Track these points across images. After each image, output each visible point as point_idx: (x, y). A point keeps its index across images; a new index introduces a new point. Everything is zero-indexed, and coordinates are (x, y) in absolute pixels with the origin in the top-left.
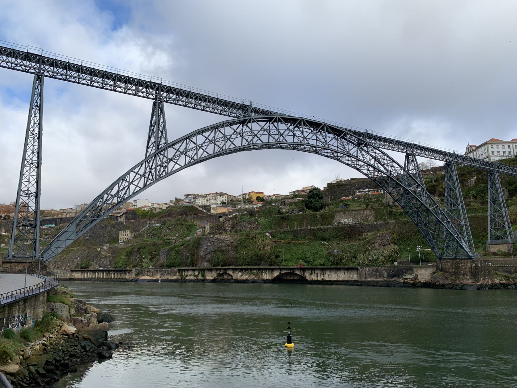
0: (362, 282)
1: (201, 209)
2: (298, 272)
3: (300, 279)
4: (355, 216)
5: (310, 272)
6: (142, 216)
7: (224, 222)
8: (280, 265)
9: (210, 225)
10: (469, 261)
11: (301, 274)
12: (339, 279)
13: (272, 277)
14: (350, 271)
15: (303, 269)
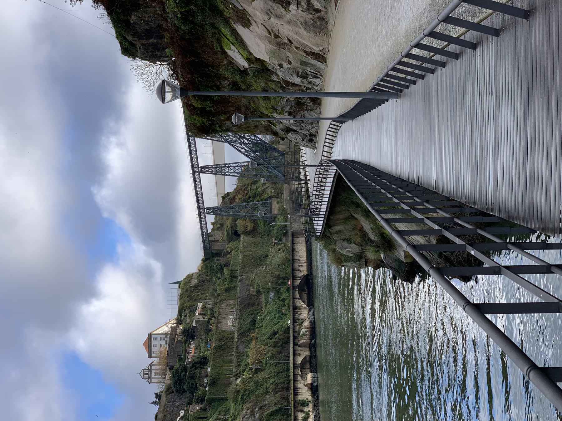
2: (298, 282)
3: (306, 293)
4: (226, 314)
5: (297, 272)
10: (286, 156)
11: (300, 279)
13: (305, 308)
14: (295, 242)
15: (294, 278)
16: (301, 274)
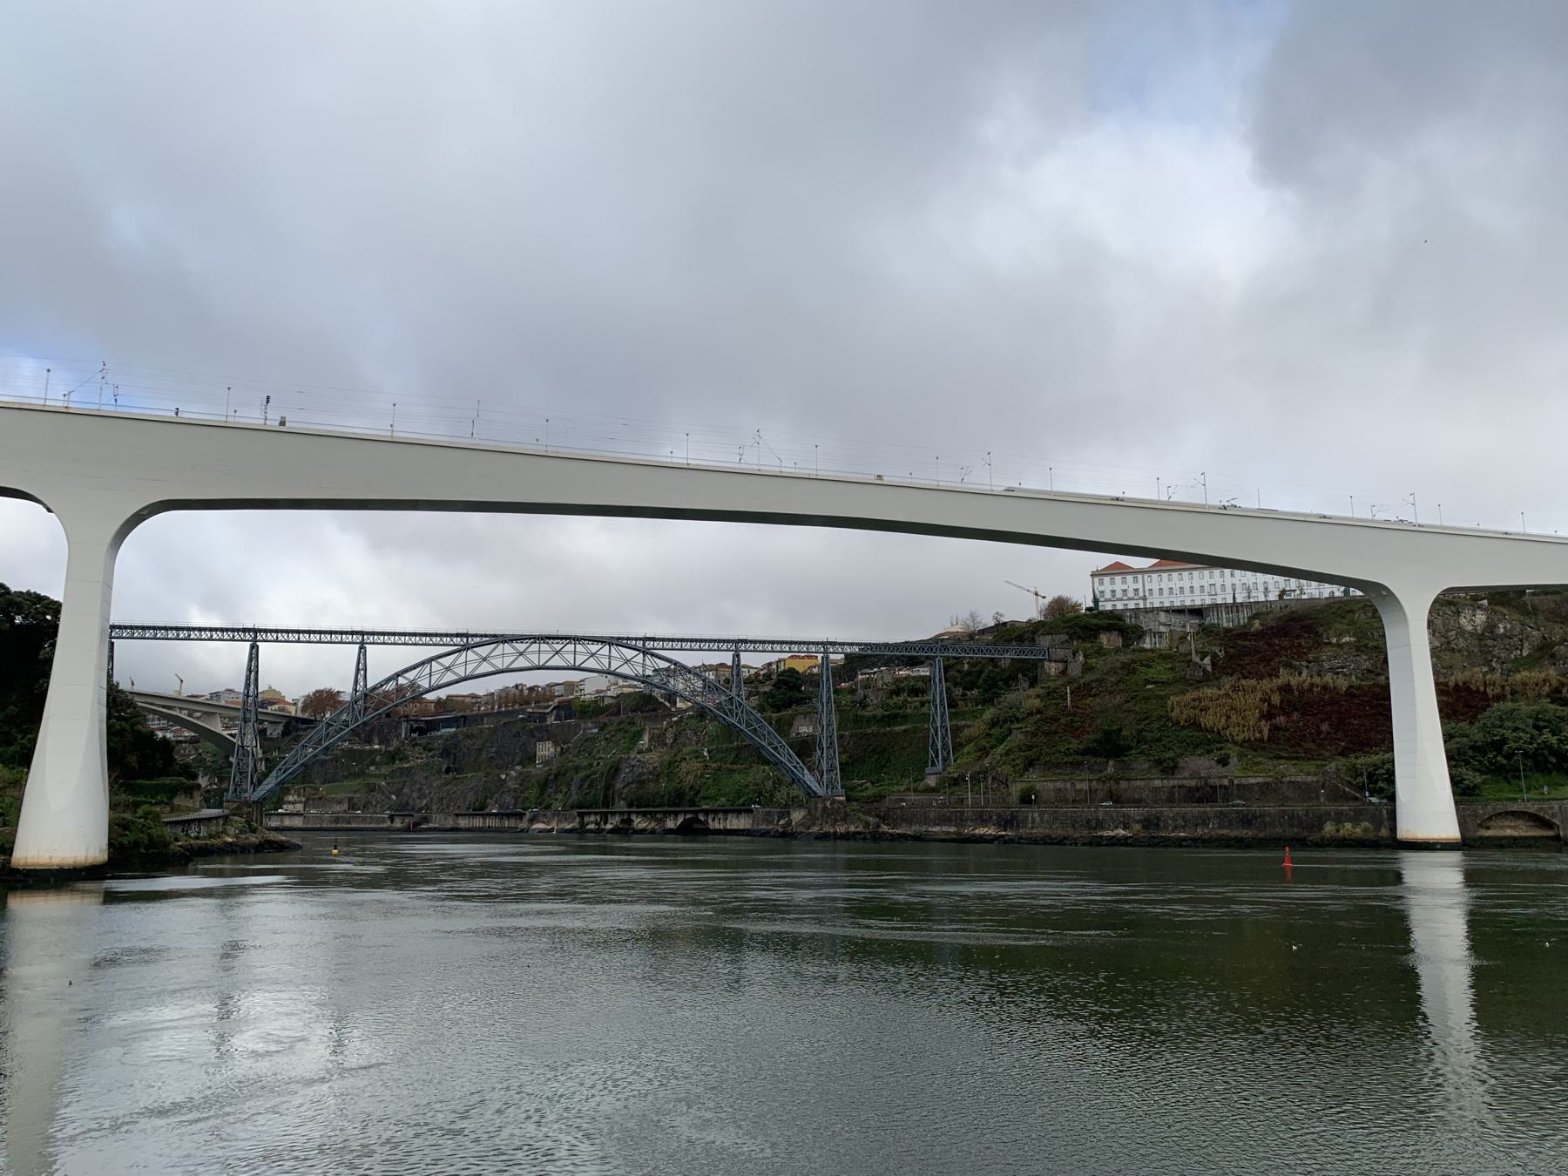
0: (754, 831)
1: (662, 700)
2: (701, 817)
5: (713, 816)
6: (581, 712)
7: (666, 730)
8: (699, 806)
9: (650, 734)
12: (740, 828)
16: (710, 821)
